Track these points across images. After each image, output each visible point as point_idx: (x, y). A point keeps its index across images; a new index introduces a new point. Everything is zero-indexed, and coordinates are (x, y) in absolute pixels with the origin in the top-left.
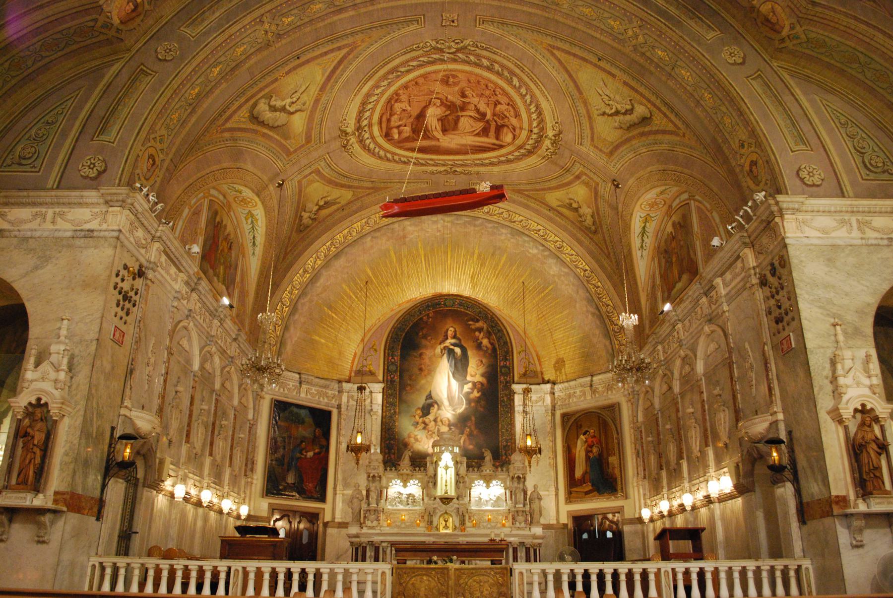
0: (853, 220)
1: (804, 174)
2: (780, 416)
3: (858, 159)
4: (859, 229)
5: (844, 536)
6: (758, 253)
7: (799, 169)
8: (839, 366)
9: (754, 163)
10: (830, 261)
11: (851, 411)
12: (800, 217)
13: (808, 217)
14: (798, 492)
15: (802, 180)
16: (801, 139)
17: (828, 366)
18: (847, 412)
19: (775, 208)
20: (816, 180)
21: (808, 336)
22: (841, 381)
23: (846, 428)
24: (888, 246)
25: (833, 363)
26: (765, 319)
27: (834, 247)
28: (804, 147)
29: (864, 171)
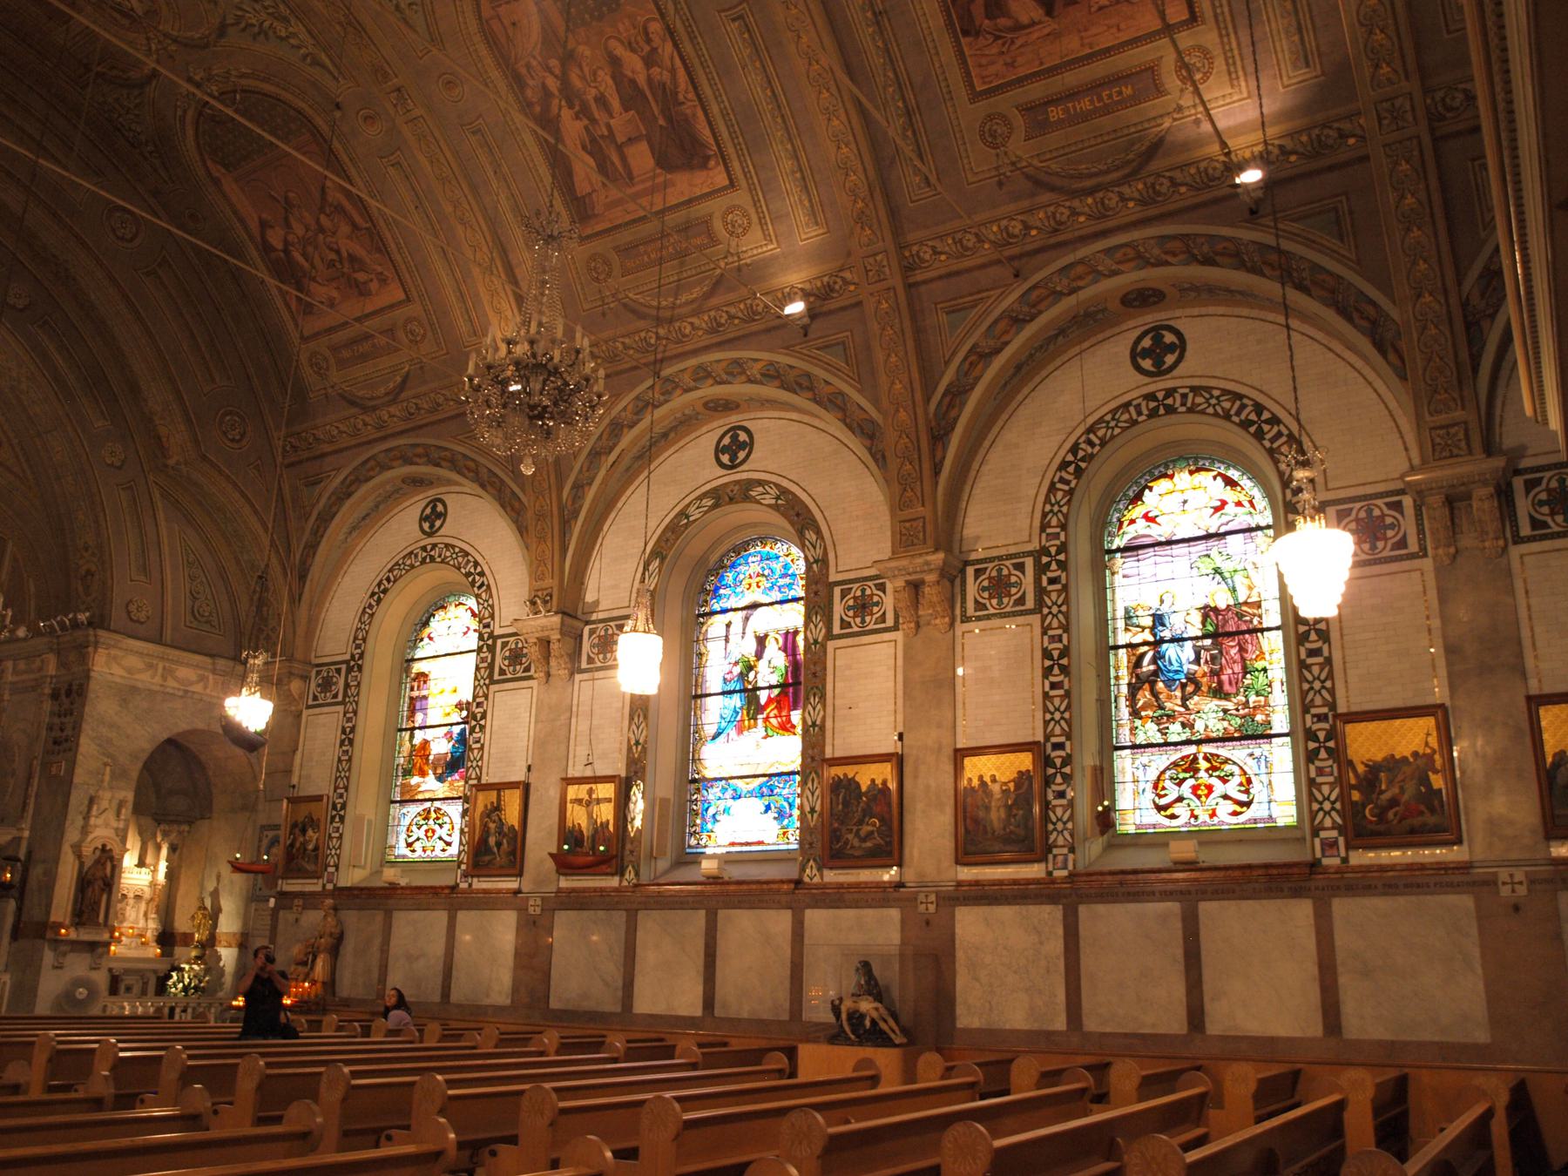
0: (161, 666)
1: (133, 608)
2: (26, 834)
3: (189, 603)
4: (164, 678)
5: (48, 956)
6: (62, 664)
7: (131, 601)
8: (95, 807)
9: (89, 572)
10: (124, 702)
11: (91, 849)
12: (113, 652)
13: (119, 653)
14: (19, 909)
15: (129, 613)
16: (145, 569)
17: (86, 802)
18: (87, 850)
19: (92, 639)
20: (142, 616)
21: (79, 771)
22: (92, 821)
23: (82, 864)
24: (182, 697)
25: (92, 801)
26: (44, 733)
27: (134, 690)
28: (143, 578)
29: (189, 617)
